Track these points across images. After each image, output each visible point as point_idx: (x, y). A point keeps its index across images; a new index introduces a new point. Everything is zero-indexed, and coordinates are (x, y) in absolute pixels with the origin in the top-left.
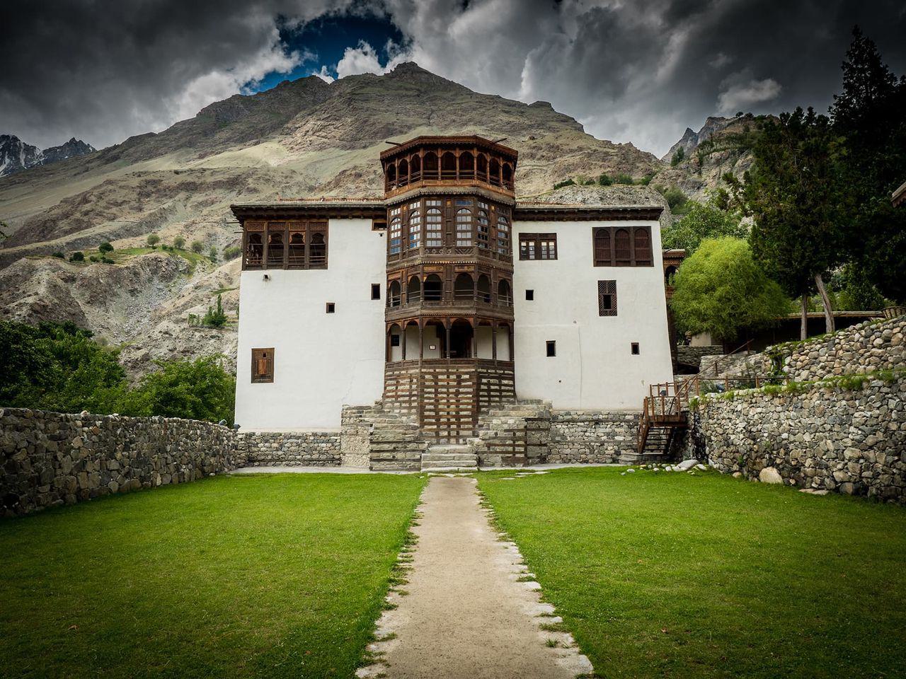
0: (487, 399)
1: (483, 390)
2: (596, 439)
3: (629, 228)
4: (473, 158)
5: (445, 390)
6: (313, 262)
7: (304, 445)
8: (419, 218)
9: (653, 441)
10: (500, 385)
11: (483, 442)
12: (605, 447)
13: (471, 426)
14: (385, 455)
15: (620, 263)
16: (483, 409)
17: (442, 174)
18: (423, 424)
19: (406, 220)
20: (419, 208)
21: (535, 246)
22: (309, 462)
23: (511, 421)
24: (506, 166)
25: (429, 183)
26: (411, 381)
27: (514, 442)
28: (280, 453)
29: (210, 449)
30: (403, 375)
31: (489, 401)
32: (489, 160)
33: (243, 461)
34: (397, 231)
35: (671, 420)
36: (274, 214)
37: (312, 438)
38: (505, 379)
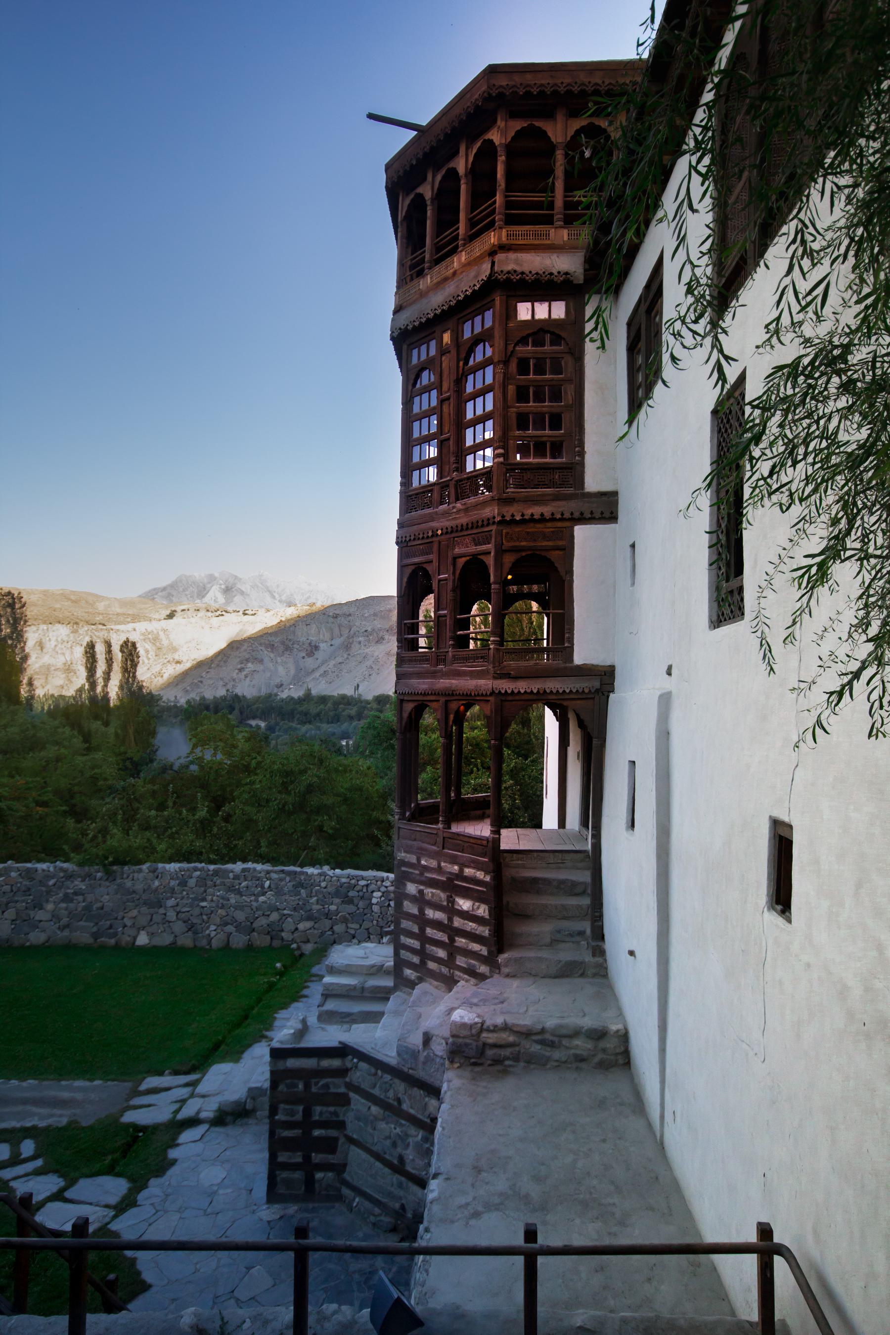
38: (466, 894)
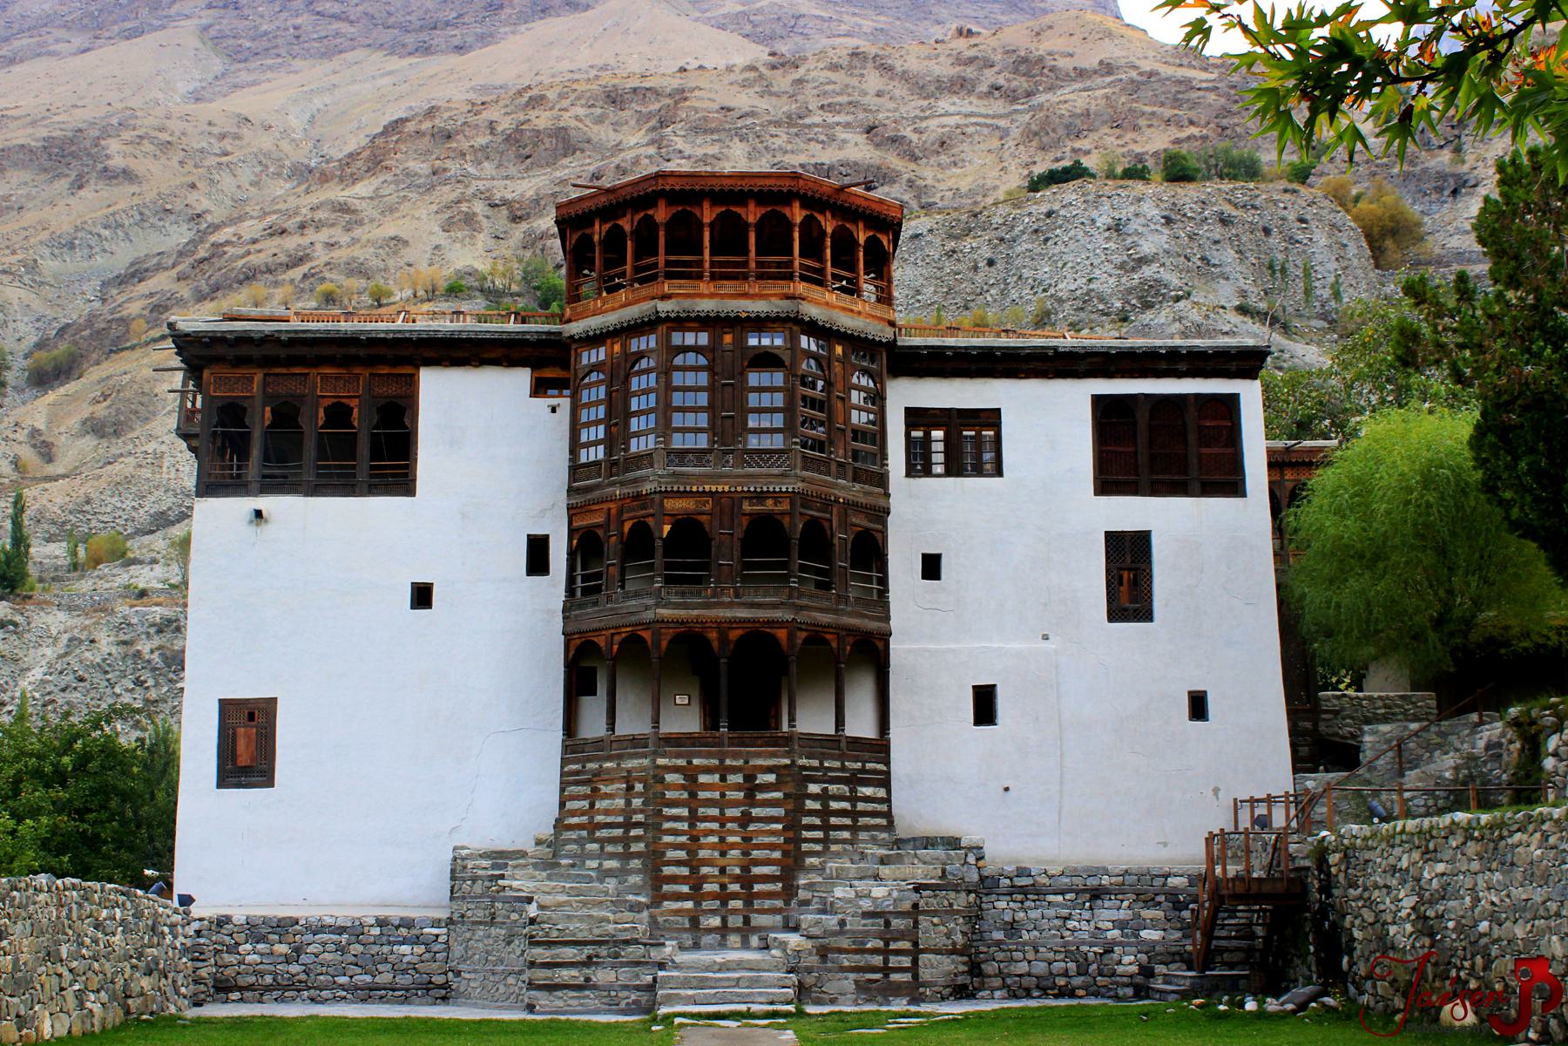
0: (819, 834)
1: (811, 813)
2: (1093, 936)
3: (1182, 398)
4: (789, 225)
5: (715, 812)
6: (377, 476)
7: (357, 948)
8: (653, 376)
9: (1235, 943)
10: (853, 799)
11: (809, 944)
12: (1115, 956)
13: (779, 903)
14: (566, 975)
15: (1157, 489)
16: (810, 861)
17: (712, 264)
18: (658, 899)
19: (619, 375)
20: (652, 351)
21: (946, 440)
22: (367, 993)
23: (879, 892)
24: (872, 243)
25: (680, 287)
26: (630, 788)
27: (887, 944)
28: (294, 968)
29: (140, 956)
30: (609, 770)
31: (825, 841)
32: (829, 230)
33: (202, 988)
34: (597, 403)
35: (1266, 888)
36: (283, 353)
37: (376, 931)
38: (866, 783)
